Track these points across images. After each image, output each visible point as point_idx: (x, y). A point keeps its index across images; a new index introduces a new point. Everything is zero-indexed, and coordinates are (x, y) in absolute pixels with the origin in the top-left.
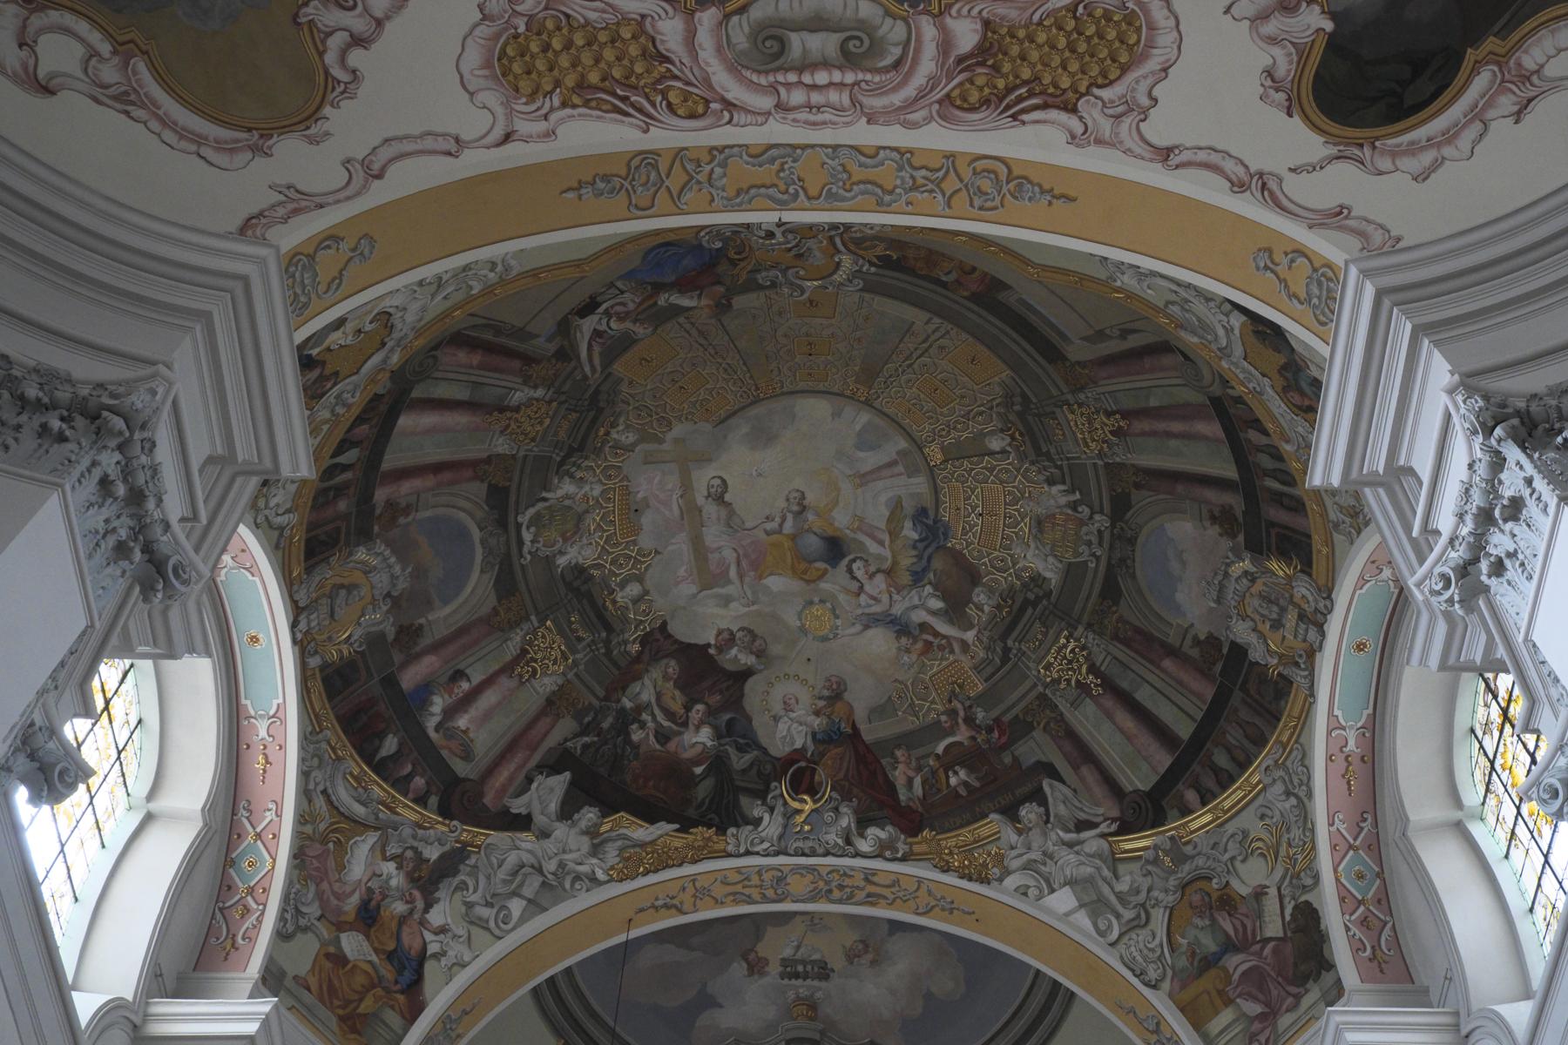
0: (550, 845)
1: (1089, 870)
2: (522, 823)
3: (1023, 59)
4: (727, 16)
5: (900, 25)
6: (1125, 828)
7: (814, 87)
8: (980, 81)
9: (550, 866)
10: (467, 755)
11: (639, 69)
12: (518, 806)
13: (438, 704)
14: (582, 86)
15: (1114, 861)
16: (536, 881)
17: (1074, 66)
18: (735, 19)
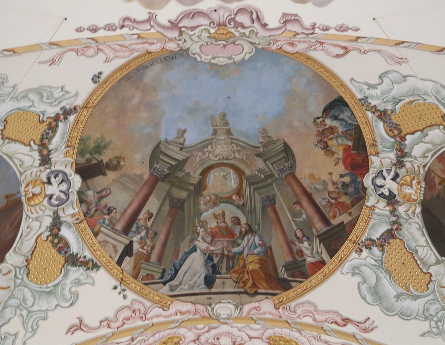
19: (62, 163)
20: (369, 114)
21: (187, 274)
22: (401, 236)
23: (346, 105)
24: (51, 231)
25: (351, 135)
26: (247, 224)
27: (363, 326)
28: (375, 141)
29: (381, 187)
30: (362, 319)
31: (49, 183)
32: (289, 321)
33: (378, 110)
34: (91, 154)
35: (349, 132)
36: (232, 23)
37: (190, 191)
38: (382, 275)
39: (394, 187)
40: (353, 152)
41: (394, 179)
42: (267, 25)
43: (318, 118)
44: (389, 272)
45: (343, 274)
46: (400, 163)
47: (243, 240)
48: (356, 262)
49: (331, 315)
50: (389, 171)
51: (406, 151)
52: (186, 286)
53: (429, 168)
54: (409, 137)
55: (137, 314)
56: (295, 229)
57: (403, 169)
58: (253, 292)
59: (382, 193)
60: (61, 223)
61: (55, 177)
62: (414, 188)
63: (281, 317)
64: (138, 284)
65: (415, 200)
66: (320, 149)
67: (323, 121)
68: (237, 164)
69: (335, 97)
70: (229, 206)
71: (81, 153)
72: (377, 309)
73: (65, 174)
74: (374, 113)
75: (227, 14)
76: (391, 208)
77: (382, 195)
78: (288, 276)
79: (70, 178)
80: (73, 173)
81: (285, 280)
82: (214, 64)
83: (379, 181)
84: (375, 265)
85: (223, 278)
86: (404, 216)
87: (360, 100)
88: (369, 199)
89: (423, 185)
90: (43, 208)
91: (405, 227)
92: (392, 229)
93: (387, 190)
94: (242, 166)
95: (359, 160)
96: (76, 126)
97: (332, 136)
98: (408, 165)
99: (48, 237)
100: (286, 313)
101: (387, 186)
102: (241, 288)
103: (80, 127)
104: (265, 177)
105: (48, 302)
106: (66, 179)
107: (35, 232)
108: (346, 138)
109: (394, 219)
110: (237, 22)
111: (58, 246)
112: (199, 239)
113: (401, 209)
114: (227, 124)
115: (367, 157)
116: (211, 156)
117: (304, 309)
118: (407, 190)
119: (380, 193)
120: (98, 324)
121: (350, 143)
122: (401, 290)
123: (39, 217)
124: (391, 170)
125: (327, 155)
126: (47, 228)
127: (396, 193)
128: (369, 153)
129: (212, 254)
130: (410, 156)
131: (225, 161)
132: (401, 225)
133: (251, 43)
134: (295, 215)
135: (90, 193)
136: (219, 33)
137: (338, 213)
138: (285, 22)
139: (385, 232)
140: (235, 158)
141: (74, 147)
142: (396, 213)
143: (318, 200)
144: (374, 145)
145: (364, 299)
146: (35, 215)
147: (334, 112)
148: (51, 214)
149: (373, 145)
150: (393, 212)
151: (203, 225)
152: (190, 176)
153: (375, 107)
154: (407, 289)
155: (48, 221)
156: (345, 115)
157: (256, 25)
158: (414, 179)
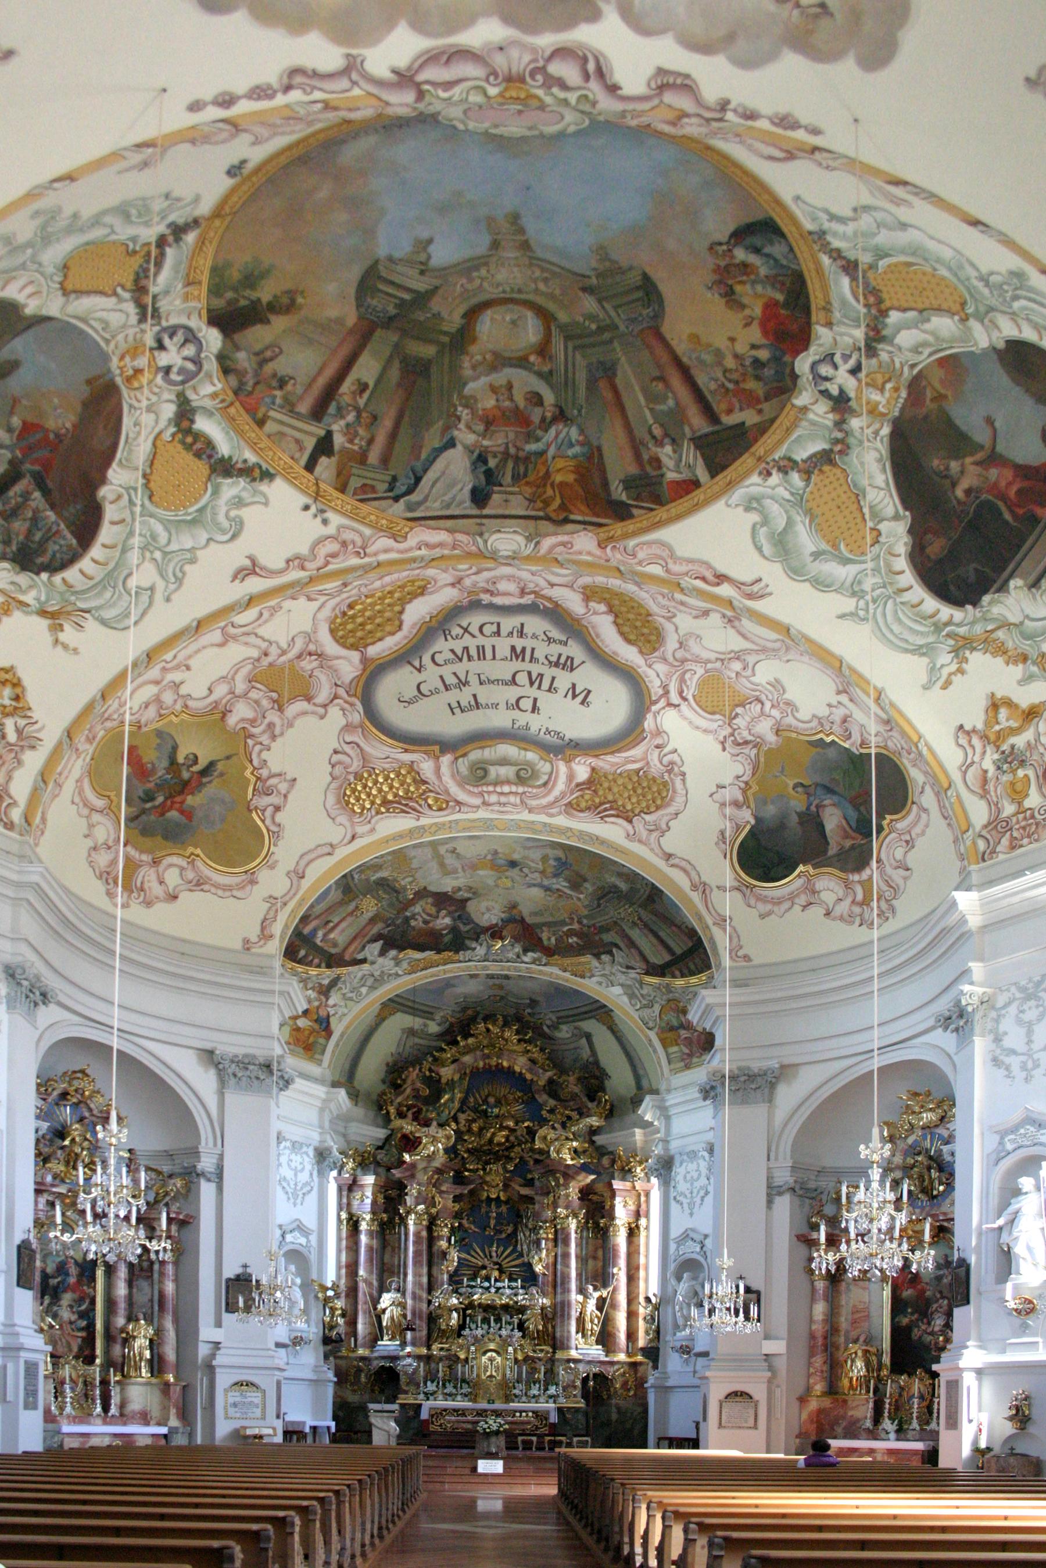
0: (376, 966)
1: (629, 983)
2: (364, 961)
3: (610, 789)
4: (456, 759)
5: (548, 765)
6: (647, 973)
7: (502, 794)
8: (587, 797)
9: (377, 974)
10: (335, 945)
11: (412, 789)
12: (360, 957)
13: (320, 934)
14: (385, 802)
15: (641, 983)
16: (372, 980)
17: (634, 800)
18: (461, 760)
19: (181, 312)
20: (825, 260)
21: (438, 485)
22: (845, 464)
23: (782, 235)
24: (177, 425)
25: (783, 284)
26: (556, 406)
27: (748, 590)
28: (829, 303)
29: (827, 379)
30: (748, 578)
31: (161, 347)
32: (622, 568)
33: (844, 258)
34: (235, 289)
35: (780, 278)
36: (539, 77)
37: (443, 345)
38: (798, 519)
39: (850, 384)
40: (782, 312)
41: (855, 371)
42: (620, 88)
43: (720, 244)
44: (812, 515)
45: (729, 506)
46: (871, 350)
47: (546, 431)
48: (755, 490)
49: (696, 567)
50: (846, 358)
51: (884, 333)
52: (437, 504)
53: (921, 371)
54: (894, 317)
55: (350, 547)
56: (651, 422)
57: (874, 361)
58: (561, 517)
59: (827, 391)
60: (193, 411)
61: (171, 337)
62: (887, 394)
63: (608, 561)
64: (348, 501)
65: (884, 415)
66: (717, 296)
67: (730, 250)
68: (541, 301)
69: (760, 216)
70: (523, 373)
71: (215, 291)
72: (777, 568)
73: (188, 329)
74: (835, 260)
75: (527, 58)
76: (837, 417)
77: (825, 393)
78: (628, 497)
79: (200, 335)
80: (204, 327)
81: (622, 504)
82: (495, 135)
83: (825, 370)
84: (788, 501)
85: (506, 493)
86: (857, 434)
87: (810, 233)
88: (800, 393)
89: (904, 394)
90: (156, 390)
91: (854, 454)
92: (831, 450)
93: (836, 387)
94: (551, 306)
95: (794, 327)
96: (201, 249)
97: (744, 278)
98: (884, 356)
99: (173, 435)
100: (618, 556)
101: (839, 380)
102: (539, 510)
103: (210, 250)
104: (598, 328)
105: (193, 537)
106: (191, 337)
107: (149, 429)
108: (773, 286)
109: (840, 435)
110: (551, 77)
111: (195, 447)
112: (462, 426)
113: (855, 423)
114: (522, 231)
115: (808, 325)
116: (485, 285)
117: (650, 551)
118: (875, 396)
119: (822, 388)
120: (282, 565)
121: (780, 297)
122: (824, 546)
123: (153, 405)
124: (850, 356)
125: (731, 308)
126: (170, 420)
127: (852, 395)
128: (814, 318)
129: (487, 452)
130: (891, 343)
131: (515, 296)
132: (848, 447)
133: (582, 112)
134: (653, 398)
135: (241, 356)
136: (507, 95)
137: (737, 406)
138: (662, 88)
139: (818, 453)
140: (536, 291)
141: (200, 283)
142: (845, 426)
143: (701, 379)
144: (827, 309)
145: (759, 549)
146: (145, 403)
147: (757, 240)
148: (173, 397)
149: (824, 308)
150: (839, 424)
151: (469, 403)
152: (442, 319)
153: (838, 251)
154: (836, 546)
155: (169, 410)
156: (777, 250)
157: (594, 85)
158: (889, 380)
